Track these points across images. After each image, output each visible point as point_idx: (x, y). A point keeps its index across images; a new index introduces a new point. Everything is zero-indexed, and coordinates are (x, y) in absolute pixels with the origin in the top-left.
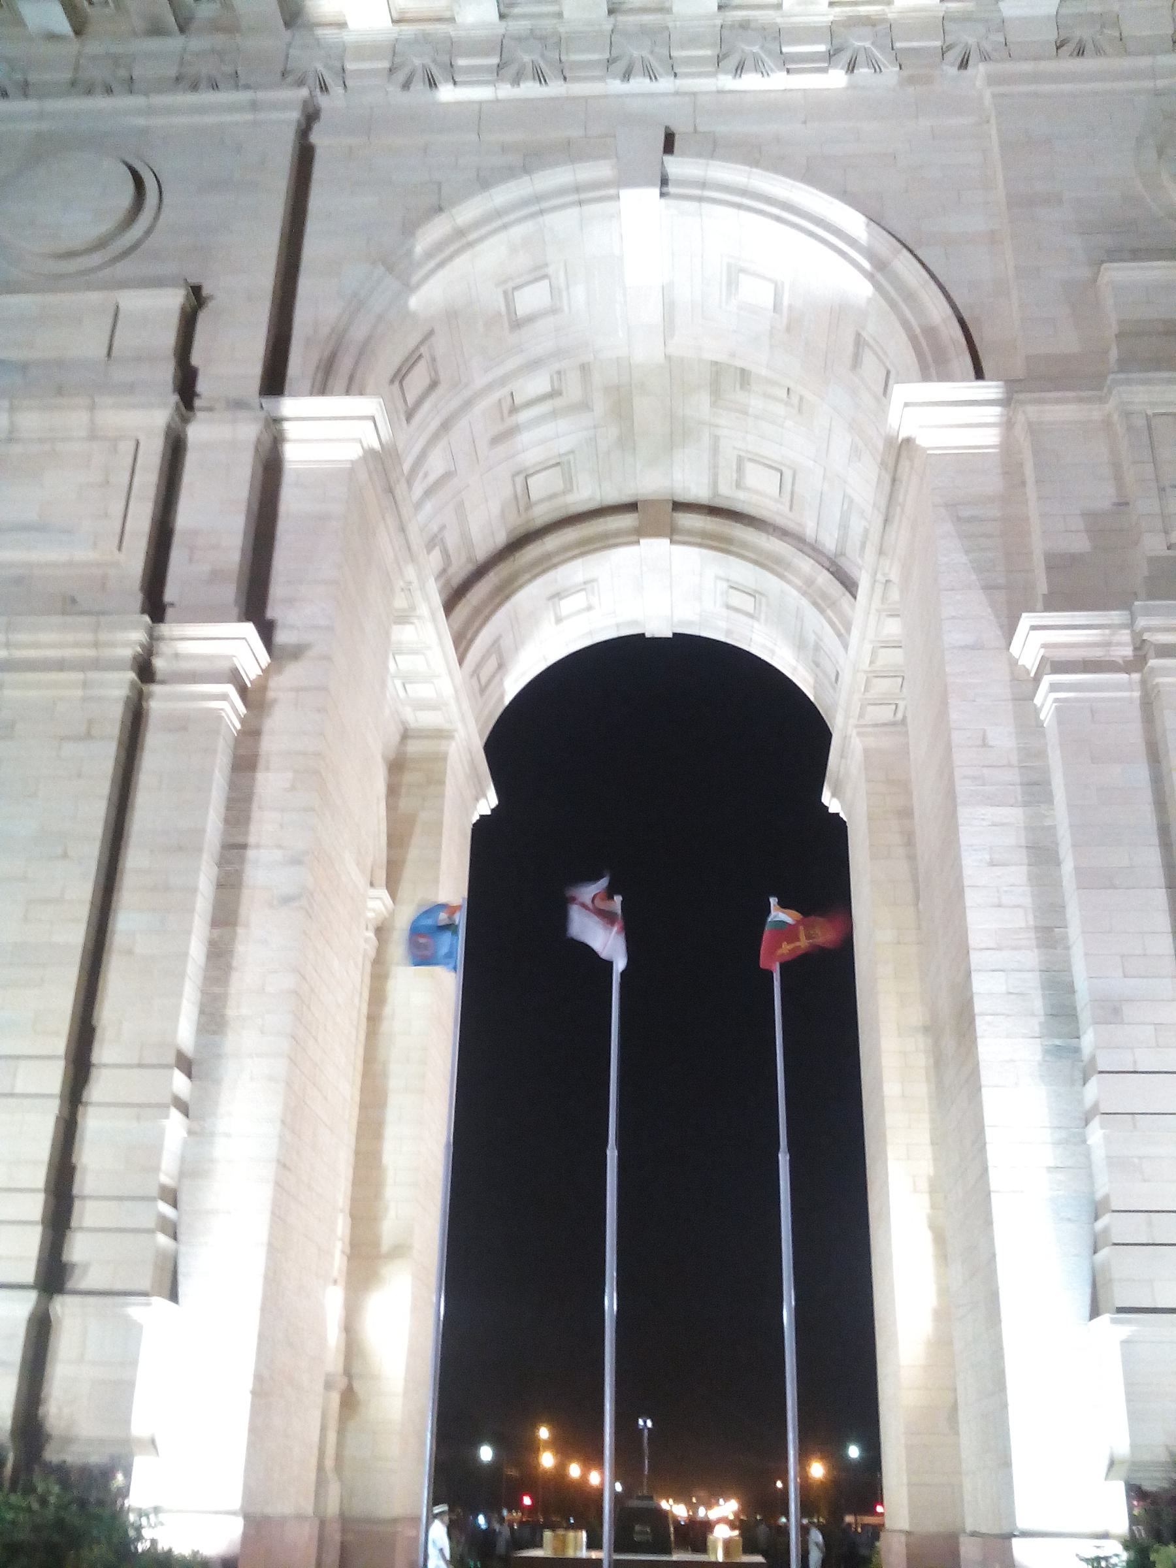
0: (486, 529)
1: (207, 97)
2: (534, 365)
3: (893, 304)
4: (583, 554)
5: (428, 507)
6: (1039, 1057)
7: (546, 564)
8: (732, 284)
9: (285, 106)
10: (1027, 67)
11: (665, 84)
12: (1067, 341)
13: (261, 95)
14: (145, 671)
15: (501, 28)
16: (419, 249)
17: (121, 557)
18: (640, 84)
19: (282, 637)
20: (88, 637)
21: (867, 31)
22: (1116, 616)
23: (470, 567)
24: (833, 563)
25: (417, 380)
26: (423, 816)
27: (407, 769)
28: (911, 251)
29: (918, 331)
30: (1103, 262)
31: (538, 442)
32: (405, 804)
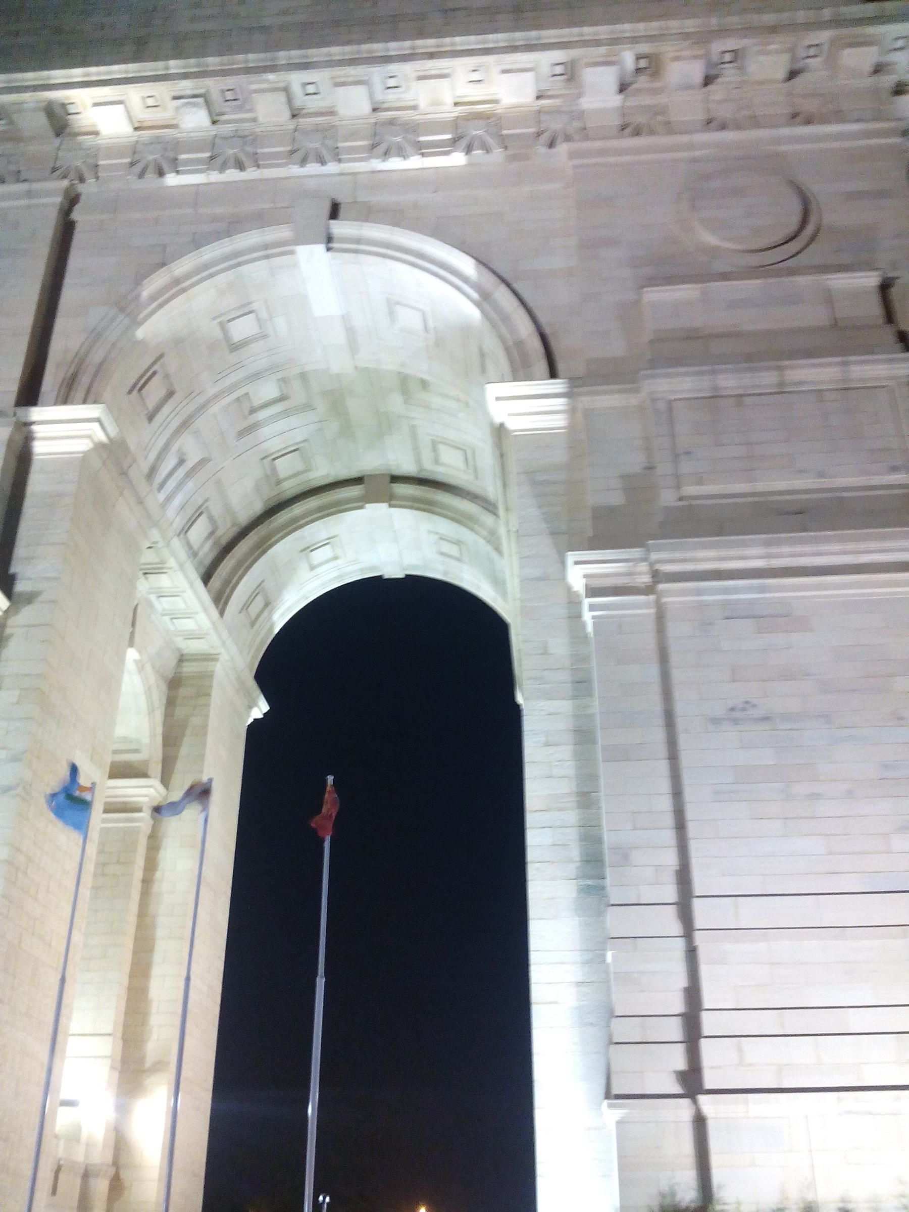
0: (243, 499)
2: (256, 376)
3: (494, 326)
5: (190, 485)
6: (574, 895)
8: (391, 314)
9: (48, 194)
10: (598, 144)
11: (332, 168)
12: (617, 347)
13: (36, 186)
15: (214, 130)
18: (313, 168)
19: (20, 587)
22: (636, 553)
25: (155, 391)
26: (195, 721)
27: (181, 687)
28: (508, 285)
29: (511, 343)
30: (644, 287)
31: (277, 434)
32: (180, 712)
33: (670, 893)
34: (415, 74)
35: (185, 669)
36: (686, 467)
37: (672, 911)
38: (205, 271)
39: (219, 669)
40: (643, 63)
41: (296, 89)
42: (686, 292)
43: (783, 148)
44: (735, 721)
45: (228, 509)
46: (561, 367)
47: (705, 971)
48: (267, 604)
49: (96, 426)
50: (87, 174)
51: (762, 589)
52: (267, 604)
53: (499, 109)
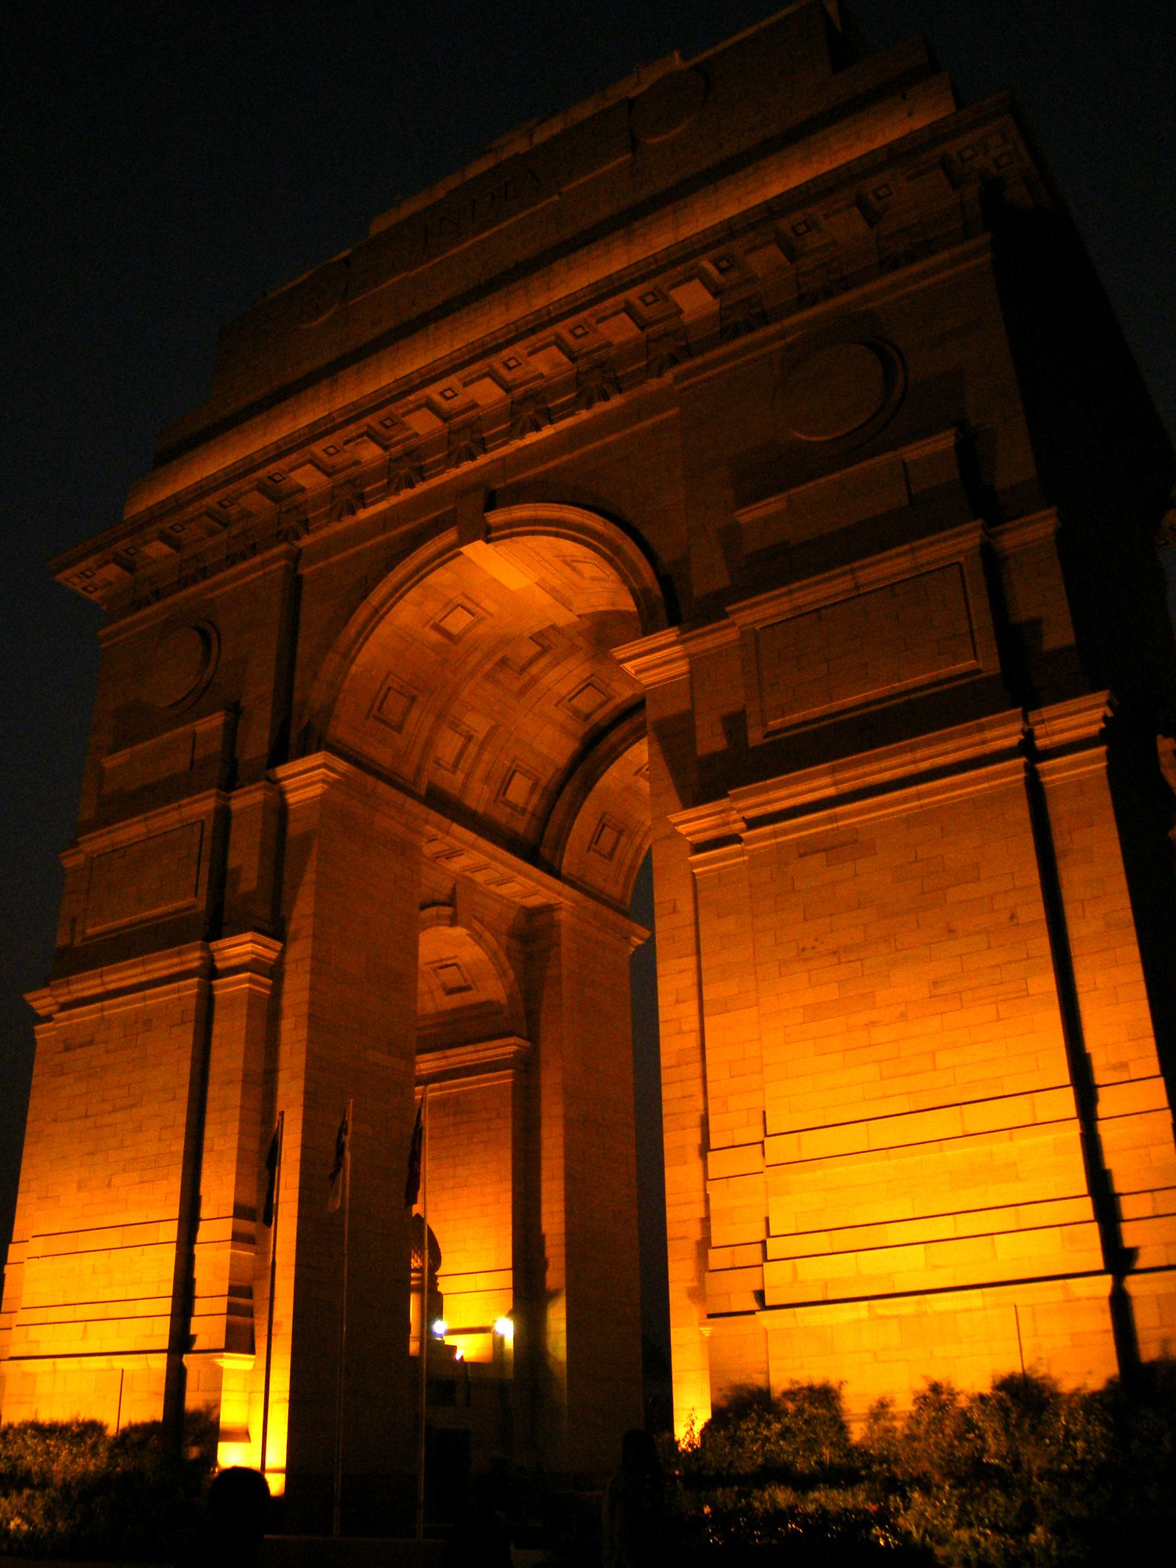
7: (614, 754)
11: (482, 460)
18: (467, 466)
34: (526, 352)
38: (397, 593)
39: (562, 915)
40: (724, 264)
41: (437, 398)
42: (772, 505)
43: (870, 305)
51: (832, 819)
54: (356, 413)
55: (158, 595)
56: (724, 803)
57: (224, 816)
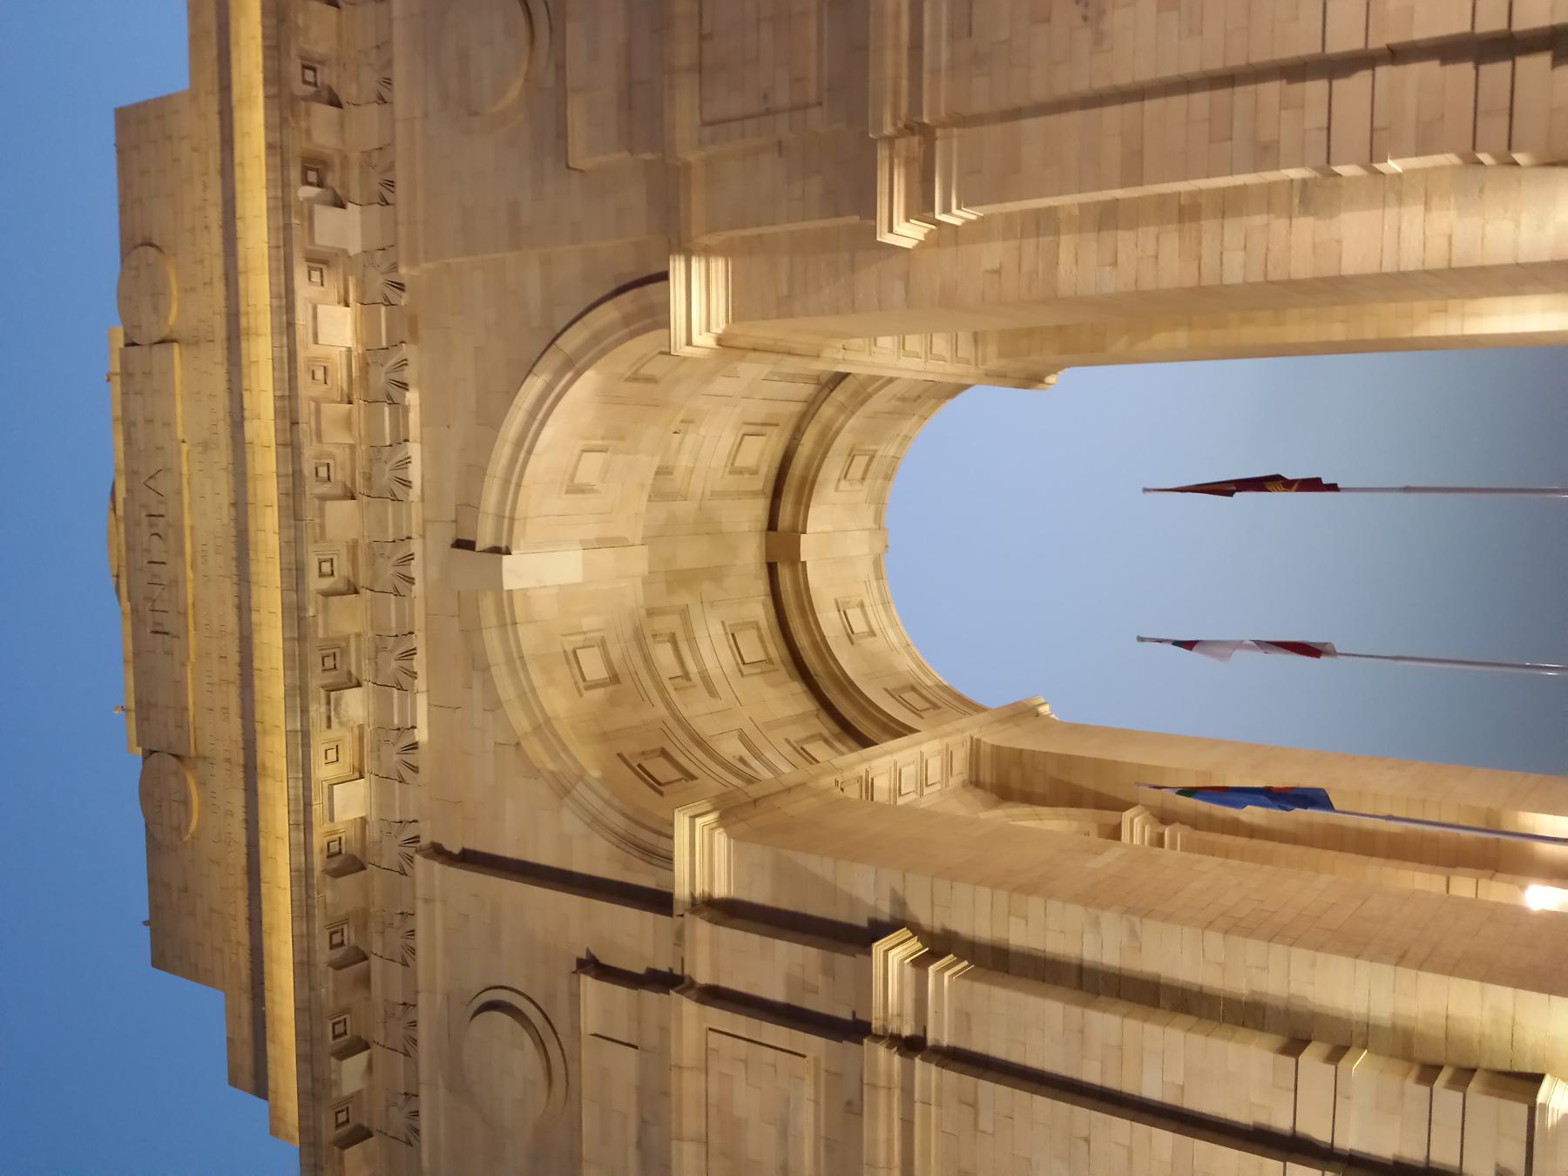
0: (788, 700)
1: (420, 941)
3: (603, 353)
4: (814, 614)
5: (770, 755)
7: (821, 647)
13: (420, 893)
14: (912, 1046)
16: (551, 766)
17: (811, 1055)
18: (415, 569)
19: (885, 911)
20: (882, 1095)
21: (373, 370)
23: (823, 716)
24: (826, 385)
28: (558, 336)
29: (626, 331)
33: (1315, 89)
34: (315, 443)
35: (988, 780)
36: (782, 98)
37: (1339, 84)
38: (528, 696)
40: (312, 176)
41: (326, 583)
44: (1101, 13)
45: (799, 719)
46: (656, 269)
47: (1423, 31)
48: (913, 689)
49: (699, 821)
50: (410, 832)
52: (913, 689)
53: (358, 350)
54: (298, 694)
55: (411, 1096)
56: (883, 153)
57: (715, 996)
